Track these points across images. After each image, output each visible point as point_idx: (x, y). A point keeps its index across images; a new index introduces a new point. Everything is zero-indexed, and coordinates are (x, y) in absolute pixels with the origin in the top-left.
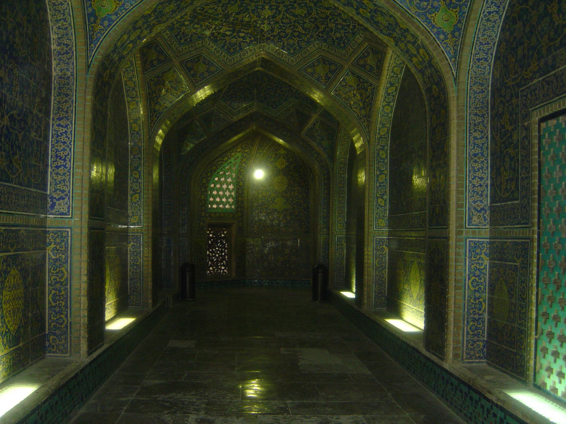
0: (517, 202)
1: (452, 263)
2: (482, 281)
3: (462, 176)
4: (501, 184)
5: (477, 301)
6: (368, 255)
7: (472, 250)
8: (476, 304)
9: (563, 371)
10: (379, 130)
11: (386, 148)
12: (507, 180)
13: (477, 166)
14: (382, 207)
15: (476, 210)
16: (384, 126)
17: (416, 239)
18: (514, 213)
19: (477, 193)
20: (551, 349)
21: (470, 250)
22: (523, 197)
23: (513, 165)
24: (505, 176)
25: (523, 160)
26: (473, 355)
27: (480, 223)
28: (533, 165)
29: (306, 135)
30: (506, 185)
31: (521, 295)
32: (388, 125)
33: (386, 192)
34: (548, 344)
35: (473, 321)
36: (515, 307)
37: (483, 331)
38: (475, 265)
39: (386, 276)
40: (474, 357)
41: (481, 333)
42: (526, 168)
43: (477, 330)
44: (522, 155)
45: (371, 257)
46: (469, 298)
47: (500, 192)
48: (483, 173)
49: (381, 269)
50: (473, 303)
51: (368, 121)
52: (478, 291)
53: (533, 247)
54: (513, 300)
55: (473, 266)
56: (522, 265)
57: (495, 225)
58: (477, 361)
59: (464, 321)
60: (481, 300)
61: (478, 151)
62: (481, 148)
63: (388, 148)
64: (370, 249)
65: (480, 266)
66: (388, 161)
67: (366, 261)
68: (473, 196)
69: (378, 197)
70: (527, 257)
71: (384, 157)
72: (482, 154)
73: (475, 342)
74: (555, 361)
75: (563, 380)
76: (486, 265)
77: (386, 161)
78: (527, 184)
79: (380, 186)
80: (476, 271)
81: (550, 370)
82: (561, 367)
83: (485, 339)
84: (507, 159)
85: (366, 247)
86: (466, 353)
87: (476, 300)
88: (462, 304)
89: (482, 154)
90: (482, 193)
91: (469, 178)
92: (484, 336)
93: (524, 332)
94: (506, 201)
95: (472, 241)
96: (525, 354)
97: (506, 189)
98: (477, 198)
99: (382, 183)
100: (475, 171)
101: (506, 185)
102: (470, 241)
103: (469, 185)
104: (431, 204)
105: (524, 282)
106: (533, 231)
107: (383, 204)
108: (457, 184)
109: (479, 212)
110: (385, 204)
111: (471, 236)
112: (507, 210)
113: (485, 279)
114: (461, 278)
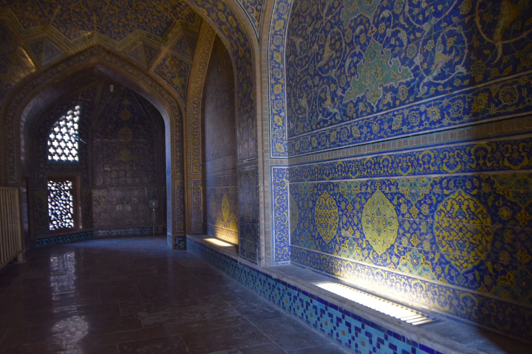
10: (274, 23)
11: (281, 49)
14: (279, 126)
16: (280, 17)
29: (155, 72)
32: (285, 17)
33: (283, 108)
39: (288, 218)
49: (281, 210)
51: (257, 11)
63: (283, 49)
64: (267, 183)
66: (284, 66)
69: (274, 115)
71: (279, 60)
77: (281, 66)
79: (276, 99)
99: (278, 95)
107: (280, 124)
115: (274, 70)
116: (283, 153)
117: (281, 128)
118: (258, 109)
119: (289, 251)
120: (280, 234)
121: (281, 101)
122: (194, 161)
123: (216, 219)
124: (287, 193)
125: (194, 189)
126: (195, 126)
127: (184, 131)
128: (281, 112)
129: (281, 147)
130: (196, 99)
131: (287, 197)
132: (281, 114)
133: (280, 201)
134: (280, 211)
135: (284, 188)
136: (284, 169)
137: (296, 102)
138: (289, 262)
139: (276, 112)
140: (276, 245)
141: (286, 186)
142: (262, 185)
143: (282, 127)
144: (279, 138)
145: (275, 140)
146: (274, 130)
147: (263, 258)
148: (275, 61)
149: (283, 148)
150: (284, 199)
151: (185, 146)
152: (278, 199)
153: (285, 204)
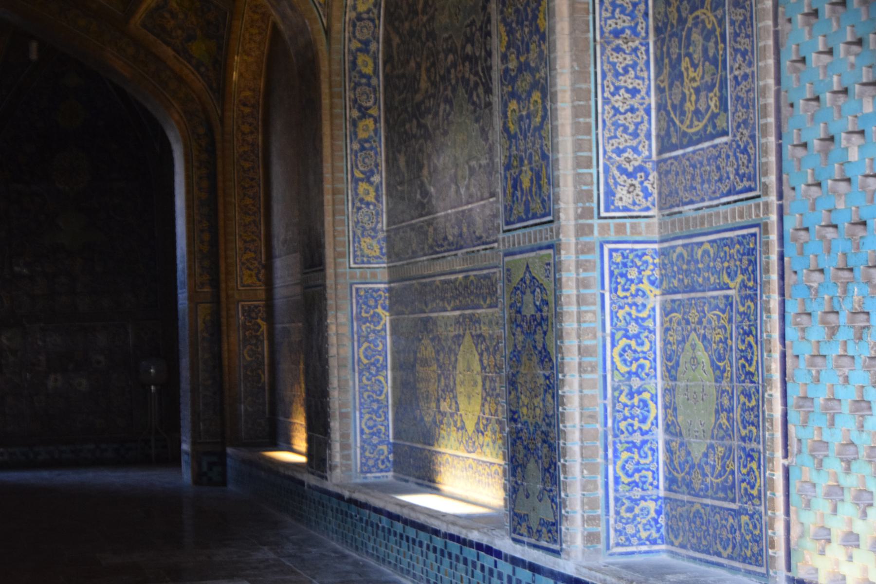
0: (724, 139)
1: (570, 308)
2: (646, 348)
3: (584, 86)
4: (683, 100)
5: (636, 400)
6: (337, 334)
7: (616, 272)
8: (633, 406)
9: (856, 530)
11: (373, 47)
12: (697, 90)
13: (621, 61)
14: (368, 204)
15: (623, 171)
17: (466, 277)
18: (718, 168)
19: (625, 129)
20: (823, 481)
21: (612, 273)
22: (739, 126)
23: (711, 53)
24: (693, 80)
25: (736, 35)
26: (634, 536)
27: (634, 204)
28: (761, 44)
30: (697, 101)
31: (744, 366)
33: (377, 165)
34: (814, 473)
35: (628, 450)
36: (731, 398)
37: (655, 473)
38: (627, 309)
40: (634, 540)
41: (650, 479)
42: (744, 54)
43: (638, 471)
44: (732, 23)
45: (347, 342)
46: (616, 394)
47: (682, 122)
48: (637, 77)
49: (373, 370)
50: (625, 405)
52: (637, 374)
53: (767, 244)
54: (725, 384)
55: (621, 314)
56: (743, 293)
57: (672, 207)
58: (644, 548)
59: (606, 450)
60: (646, 396)
61: (623, 22)
62: (632, 15)
63: (378, 47)
64: (343, 318)
65: (638, 311)
66: (379, 81)
67: (333, 351)
68: (615, 137)
70: (754, 271)
71: (369, 70)
72: (634, 30)
73: (635, 502)
74: (835, 511)
75: (855, 552)
76: (654, 309)
77: (374, 81)
78: (748, 92)
79: (363, 149)
80: (628, 324)
81: (824, 537)
82: (850, 522)
83: (662, 493)
84: (696, 37)
85: (331, 313)
86: (616, 531)
87: (632, 398)
88: (600, 410)
89: (634, 30)
90: (637, 128)
91: (603, 91)
92: (657, 487)
93: (755, 455)
94: (699, 142)
95: (616, 250)
96: (762, 509)
97: (697, 112)
98: (623, 140)
99: (367, 141)
100: (617, 75)
101: (697, 101)
102: (611, 251)
103: (604, 110)
104: (508, 167)
105: (749, 333)
106: (766, 205)
107: (371, 198)
108: (574, 107)
109: (630, 175)
110: (378, 198)
111: (613, 237)
112: (701, 163)
113: (652, 343)
114: (593, 342)
115: (358, 90)
116: (377, 257)
117: (371, 207)
118: (325, 170)
119: (389, 453)
120: (371, 419)
121: (372, 153)
122: (245, 257)
123: (291, 403)
124: (385, 338)
125: (246, 328)
126: (247, 165)
127: (220, 178)
128: (372, 173)
129: (373, 246)
130: (248, 93)
131: (385, 345)
132: (372, 179)
133: (369, 353)
134: (371, 374)
135: (379, 328)
136: (379, 290)
137: (395, 159)
138: (390, 474)
139: (362, 176)
140: (363, 441)
141: (382, 323)
142: (333, 321)
143: (375, 205)
144: (367, 227)
145: (359, 232)
146: (357, 212)
147: (336, 466)
148: (360, 72)
149: (376, 247)
150: (380, 348)
151: (221, 215)
152: (366, 349)
153: (381, 359)
